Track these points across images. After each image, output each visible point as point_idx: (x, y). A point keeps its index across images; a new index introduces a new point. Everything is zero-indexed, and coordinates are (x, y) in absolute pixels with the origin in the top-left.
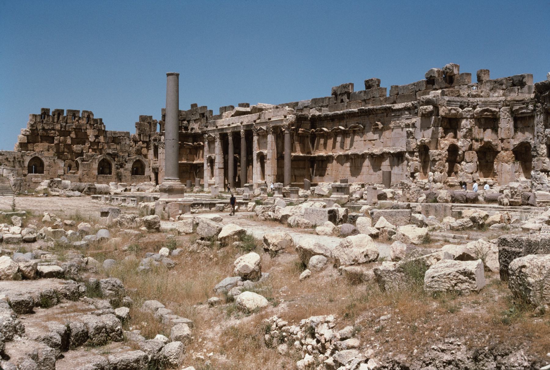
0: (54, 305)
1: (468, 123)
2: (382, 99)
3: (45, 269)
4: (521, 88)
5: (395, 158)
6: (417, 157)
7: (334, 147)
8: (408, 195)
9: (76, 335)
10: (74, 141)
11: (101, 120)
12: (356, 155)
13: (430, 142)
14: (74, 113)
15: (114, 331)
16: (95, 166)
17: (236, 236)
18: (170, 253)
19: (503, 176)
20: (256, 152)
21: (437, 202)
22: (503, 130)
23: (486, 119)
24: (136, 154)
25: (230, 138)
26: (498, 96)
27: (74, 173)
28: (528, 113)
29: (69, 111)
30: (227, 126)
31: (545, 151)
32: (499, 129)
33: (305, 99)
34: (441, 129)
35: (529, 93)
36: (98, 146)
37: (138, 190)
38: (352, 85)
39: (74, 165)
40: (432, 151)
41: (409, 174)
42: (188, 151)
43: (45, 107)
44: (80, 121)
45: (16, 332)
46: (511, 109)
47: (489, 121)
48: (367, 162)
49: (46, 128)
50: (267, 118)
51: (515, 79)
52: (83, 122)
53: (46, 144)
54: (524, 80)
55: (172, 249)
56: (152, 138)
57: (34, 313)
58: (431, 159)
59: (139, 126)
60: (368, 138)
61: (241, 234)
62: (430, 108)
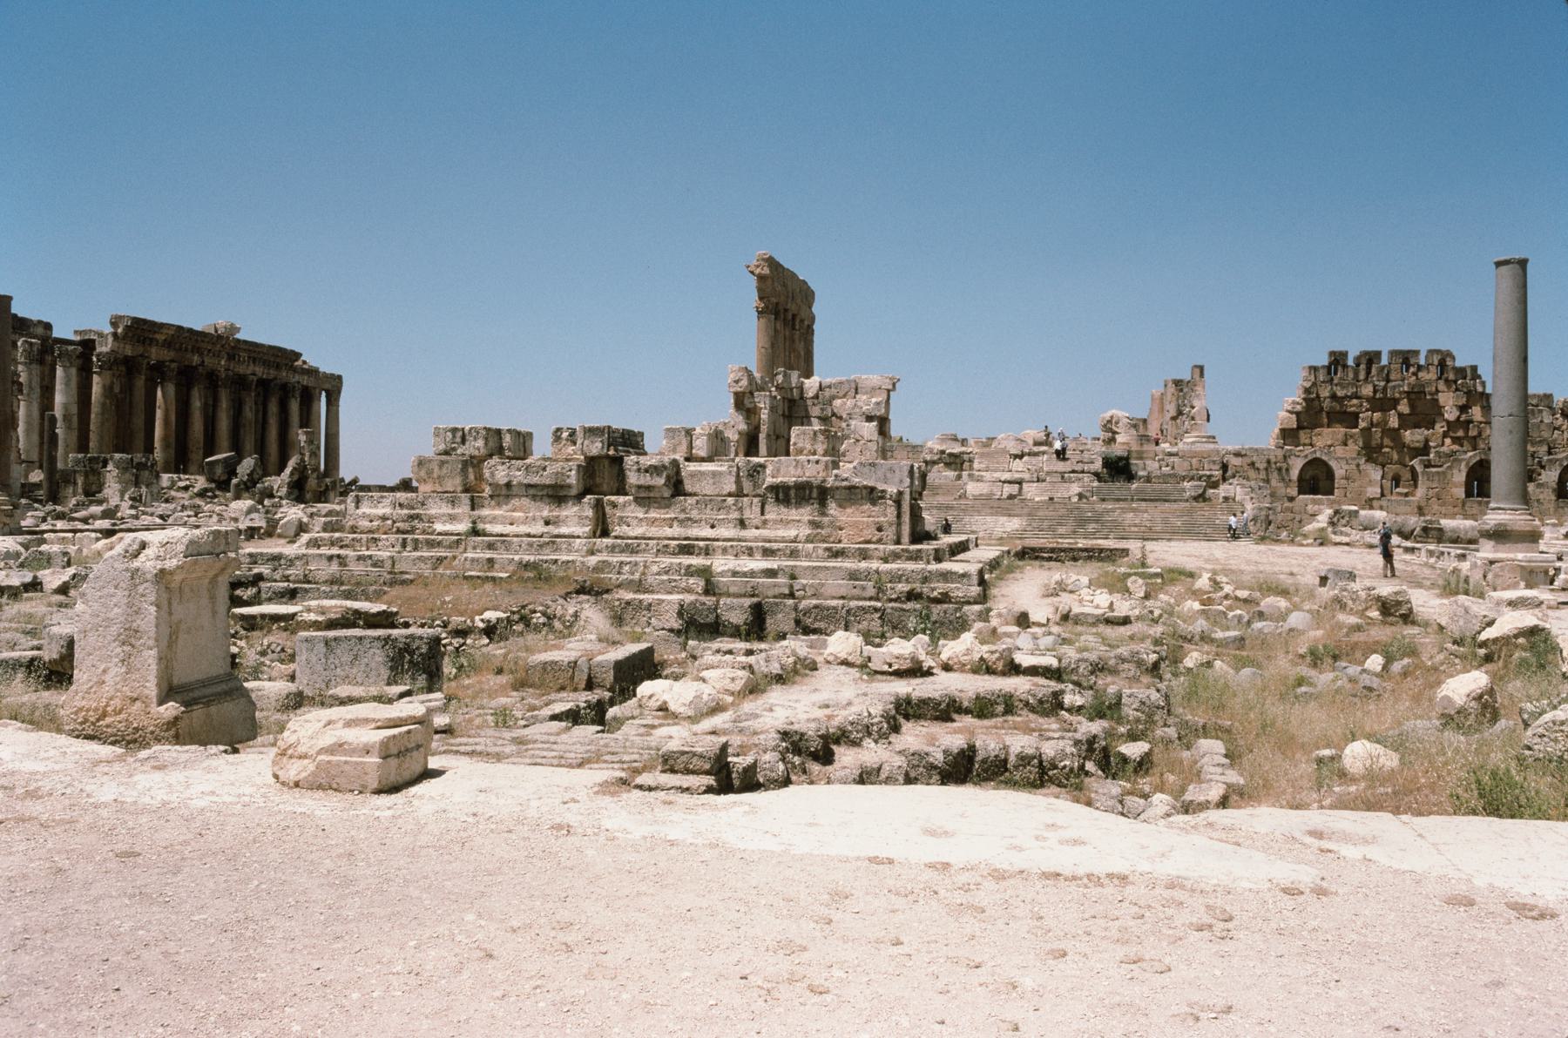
3: (1024, 660)
9: (984, 761)
10: (1405, 422)
11: (1474, 368)
14: (1406, 358)
15: (1056, 767)
16: (1460, 476)
17: (1521, 640)
18: (1385, 667)
27: (1406, 495)
29: (1393, 353)
36: (1467, 430)
39: (1406, 475)
44: (1420, 374)
45: (869, 734)
49: (1340, 393)
52: (1430, 375)
53: (1341, 431)
55: (1389, 660)
57: (953, 721)
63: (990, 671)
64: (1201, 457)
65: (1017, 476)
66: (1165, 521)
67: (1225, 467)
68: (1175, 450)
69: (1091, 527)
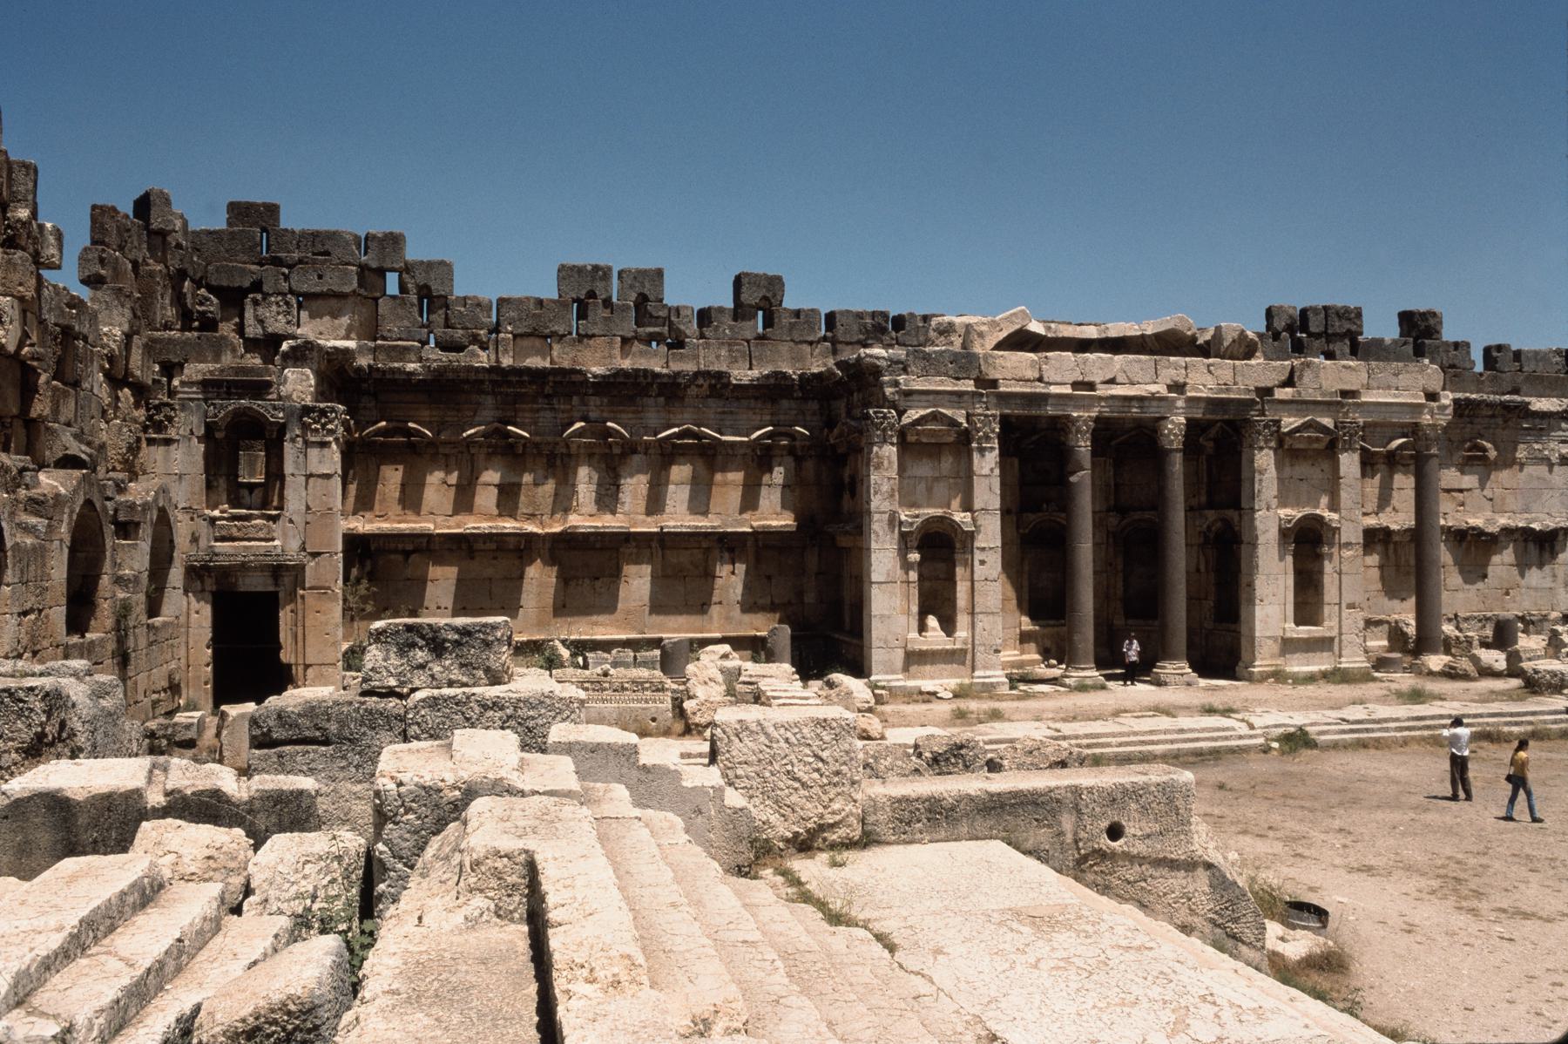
5: (1531, 546)
30: (1067, 390)
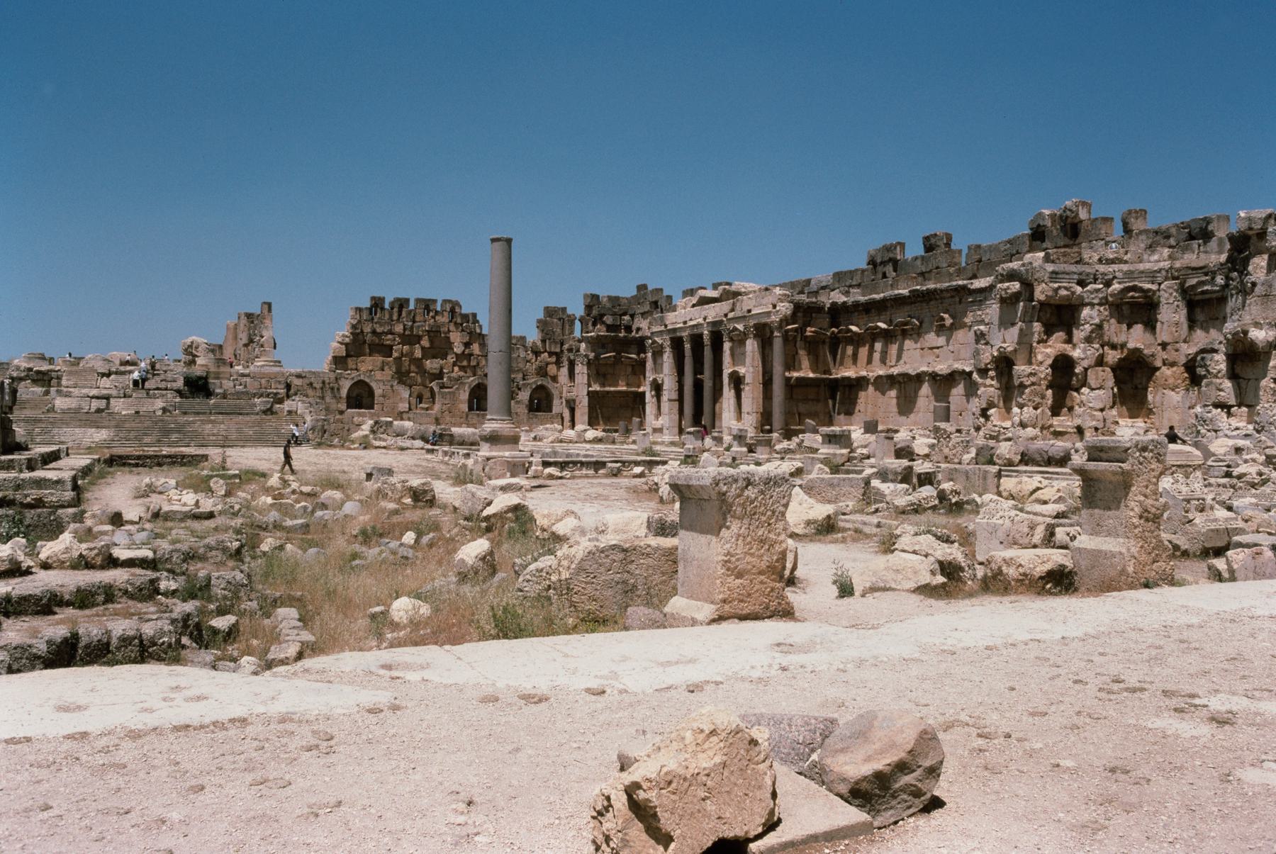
0: (98, 605)
1: (1095, 313)
2: (952, 270)
3: (122, 554)
4: (1205, 243)
6: (992, 379)
7: (870, 361)
8: (946, 451)
9: (87, 646)
10: (427, 353)
11: (474, 315)
12: (905, 376)
13: (1015, 350)
14: (427, 305)
15: (155, 644)
16: (464, 395)
17: (510, 515)
18: (417, 541)
19: (1166, 415)
20: (727, 371)
21: (995, 464)
22: (1165, 326)
23: (1133, 305)
24: (538, 374)
25: (687, 346)
26: (1159, 260)
27: (427, 409)
28: (1215, 292)
29: (418, 301)
31: (1223, 366)
32: (1159, 325)
33: (821, 275)
34: (1037, 327)
35: (1220, 252)
37: (535, 439)
38: (902, 245)
39: (427, 394)
40: (1020, 369)
41: (978, 412)
42: (630, 369)
43: (377, 294)
46: (1182, 285)
47: (1139, 309)
48: (926, 389)
49: (379, 330)
50: (745, 309)
51: (1193, 226)
52: (443, 319)
53: (379, 359)
54: (1210, 228)
55: (420, 535)
56: (566, 346)
57: (55, 613)
58: (1016, 383)
59: (542, 325)
60: (928, 345)
61: (518, 510)
62: (1015, 286)
63: (89, 566)
64: (270, 378)
65: (105, 392)
66: (239, 431)
67: (288, 386)
68: (247, 371)
69: (174, 437)
